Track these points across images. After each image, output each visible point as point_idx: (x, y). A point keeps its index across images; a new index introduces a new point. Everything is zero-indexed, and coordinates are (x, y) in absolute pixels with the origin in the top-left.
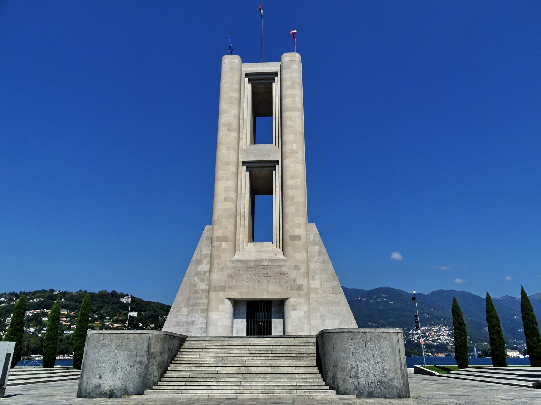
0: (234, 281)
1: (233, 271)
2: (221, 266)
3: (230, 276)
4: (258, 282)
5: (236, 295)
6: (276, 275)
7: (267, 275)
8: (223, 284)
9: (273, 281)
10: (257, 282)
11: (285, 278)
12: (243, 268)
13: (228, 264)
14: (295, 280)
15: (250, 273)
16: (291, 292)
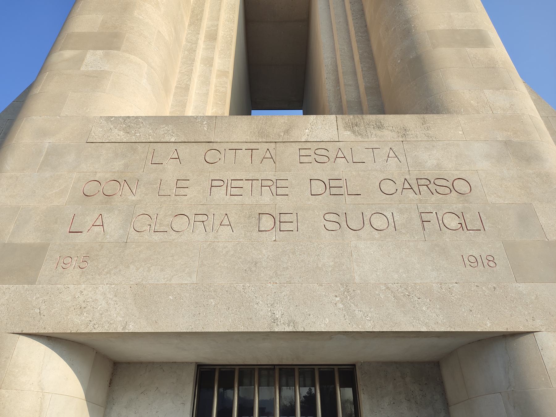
0: (113, 225)
1: (118, 165)
2: (47, 142)
3: (91, 188)
4: (278, 221)
5: (108, 308)
6: (388, 187)
7: (332, 187)
8: (29, 236)
9: (379, 222)
10: (267, 222)
11: (454, 202)
12: (184, 150)
13: (98, 134)
14: (526, 217)
15: (228, 175)
16: (522, 287)
